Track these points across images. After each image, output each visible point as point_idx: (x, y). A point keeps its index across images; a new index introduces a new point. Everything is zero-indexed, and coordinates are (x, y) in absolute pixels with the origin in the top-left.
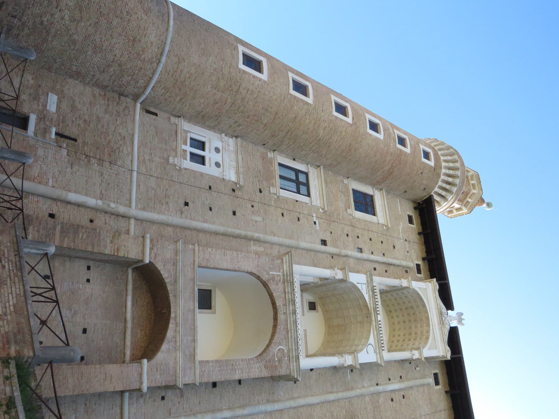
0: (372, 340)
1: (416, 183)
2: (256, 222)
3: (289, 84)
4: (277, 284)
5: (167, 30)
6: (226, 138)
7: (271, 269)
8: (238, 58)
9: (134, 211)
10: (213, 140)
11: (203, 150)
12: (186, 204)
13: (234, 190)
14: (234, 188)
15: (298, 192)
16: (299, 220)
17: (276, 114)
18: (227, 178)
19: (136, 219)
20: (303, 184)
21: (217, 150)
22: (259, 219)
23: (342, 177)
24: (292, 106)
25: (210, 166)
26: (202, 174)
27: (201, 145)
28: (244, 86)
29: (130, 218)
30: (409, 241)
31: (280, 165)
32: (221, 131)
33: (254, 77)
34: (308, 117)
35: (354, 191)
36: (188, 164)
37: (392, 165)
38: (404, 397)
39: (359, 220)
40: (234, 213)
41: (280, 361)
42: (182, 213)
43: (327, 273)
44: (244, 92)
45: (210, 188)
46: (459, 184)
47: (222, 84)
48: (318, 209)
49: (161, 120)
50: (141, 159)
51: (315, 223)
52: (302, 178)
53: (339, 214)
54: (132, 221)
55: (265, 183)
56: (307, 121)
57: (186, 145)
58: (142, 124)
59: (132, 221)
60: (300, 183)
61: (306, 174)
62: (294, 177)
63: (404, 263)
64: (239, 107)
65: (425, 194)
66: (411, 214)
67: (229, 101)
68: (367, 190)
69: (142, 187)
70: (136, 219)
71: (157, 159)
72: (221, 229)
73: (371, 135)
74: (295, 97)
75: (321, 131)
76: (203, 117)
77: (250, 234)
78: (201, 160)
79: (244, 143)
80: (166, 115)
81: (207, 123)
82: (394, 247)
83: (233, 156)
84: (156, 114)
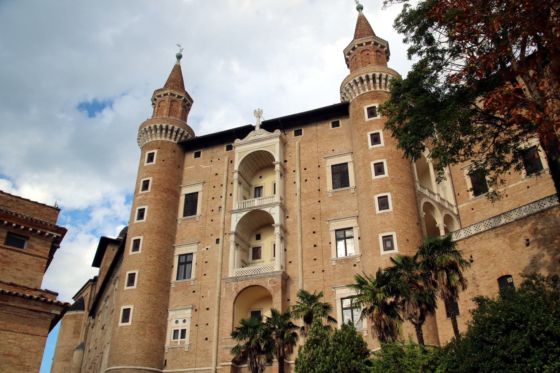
0: (267, 210)
1: (171, 163)
3: (132, 289)
4: (238, 286)
5: (124, 369)
7: (231, 291)
8: (126, 326)
9: (213, 368)
10: (171, 327)
11: (178, 330)
12: (206, 339)
13: (196, 310)
14: (194, 310)
15: (191, 262)
16: (206, 262)
17: (149, 294)
19: (217, 366)
21: (177, 322)
22: (209, 292)
23: (178, 225)
24: (143, 285)
25: (185, 326)
26: (191, 331)
28: (139, 319)
29: (216, 369)
30: (212, 157)
31: (177, 279)
32: (166, 321)
33: (133, 314)
34: (146, 272)
35: (184, 215)
36: (187, 340)
37: (162, 192)
38: (305, 169)
39: (202, 209)
40: (208, 309)
41: (275, 283)
42: (211, 341)
43: (232, 247)
44: (143, 318)
45: (197, 325)
46: (165, 123)
47: (142, 333)
48: (199, 247)
49: (167, 357)
50: (189, 366)
51: (207, 249)
52: (183, 259)
53: (200, 228)
54: (217, 368)
55: (189, 289)
56: (149, 271)
58: (172, 368)
59: (217, 368)
61: (180, 256)
62: (184, 266)
64: (151, 318)
65: (178, 149)
66: (193, 155)
67: (149, 325)
68: (182, 199)
69: (202, 364)
70: (217, 366)
71: (187, 358)
72: (216, 318)
73: (147, 218)
75: (153, 259)
76: (161, 336)
77: (217, 300)
80: (165, 355)
81: (164, 331)
82: (217, 174)
83: (178, 312)
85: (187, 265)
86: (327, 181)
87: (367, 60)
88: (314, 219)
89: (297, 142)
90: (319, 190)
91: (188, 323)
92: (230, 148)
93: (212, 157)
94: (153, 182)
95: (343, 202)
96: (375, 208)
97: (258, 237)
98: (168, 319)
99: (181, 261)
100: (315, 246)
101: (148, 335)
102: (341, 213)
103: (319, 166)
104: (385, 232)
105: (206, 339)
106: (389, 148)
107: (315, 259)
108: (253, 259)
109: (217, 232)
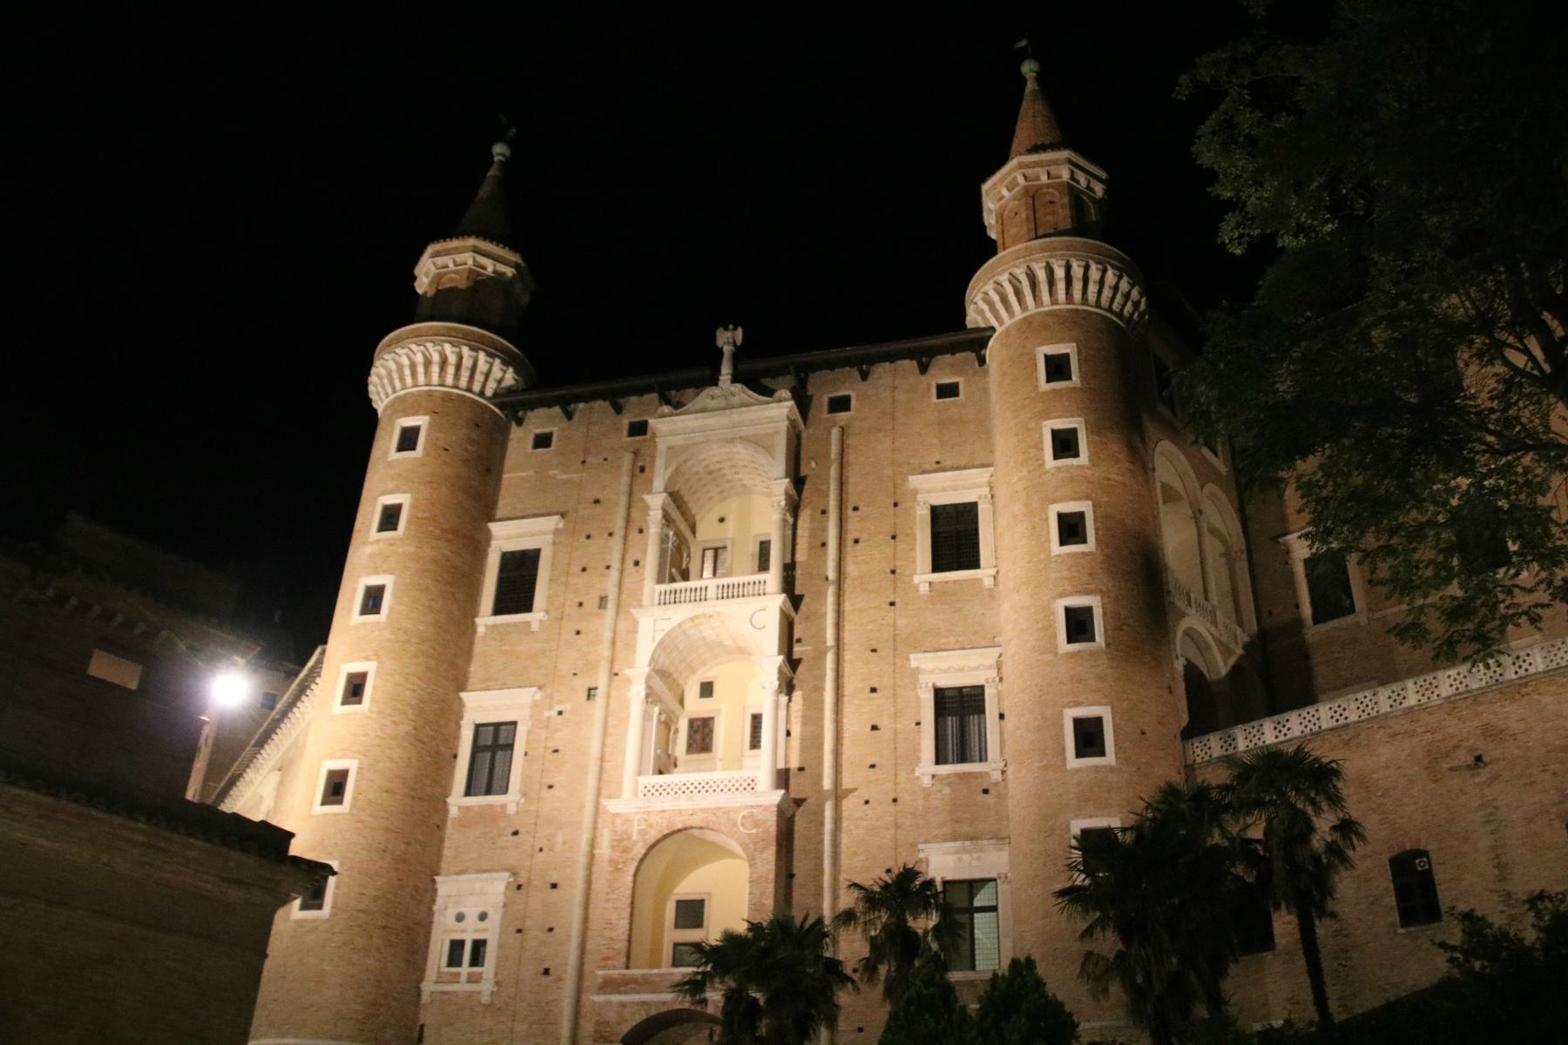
2: (565, 843)
6: (439, 901)
12: (547, 972)
13: (519, 887)
18: (501, 899)
20: (496, 735)
21: (460, 918)
25: (485, 930)
26: (501, 947)
27: (457, 946)
32: (431, 913)
36: (488, 969)
38: (856, 509)
40: (554, 886)
45: (519, 931)
49: (428, 1017)
51: (560, 713)
57: (459, 974)
60: (495, 743)
61: (478, 727)
63: (625, 479)
73: (391, 608)
74: (354, 798)
78: (479, 945)
79: (444, 865)
84: (422, 1026)
85: (499, 754)
86: (918, 547)
87: (1050, 218)
88: (874, 651)
89: (835, 432)
90: (893, 572)
91: (495, 917)
92: (639, 429)
93: (587, 451)
94: (414, 507)
95: (960, 610)
96: (1055, 636)
97: (707, 690)
98: (435, 908)
99: (481, 742)
100: (874, 728)
101: (378, 950)
102: (952, 639)
103: (896, 505)
104: (1078, 704)
105: (547, 972)
106: (1099, 472)
107: (873, 766)
108: (691, 748)
109: (591, 667)
